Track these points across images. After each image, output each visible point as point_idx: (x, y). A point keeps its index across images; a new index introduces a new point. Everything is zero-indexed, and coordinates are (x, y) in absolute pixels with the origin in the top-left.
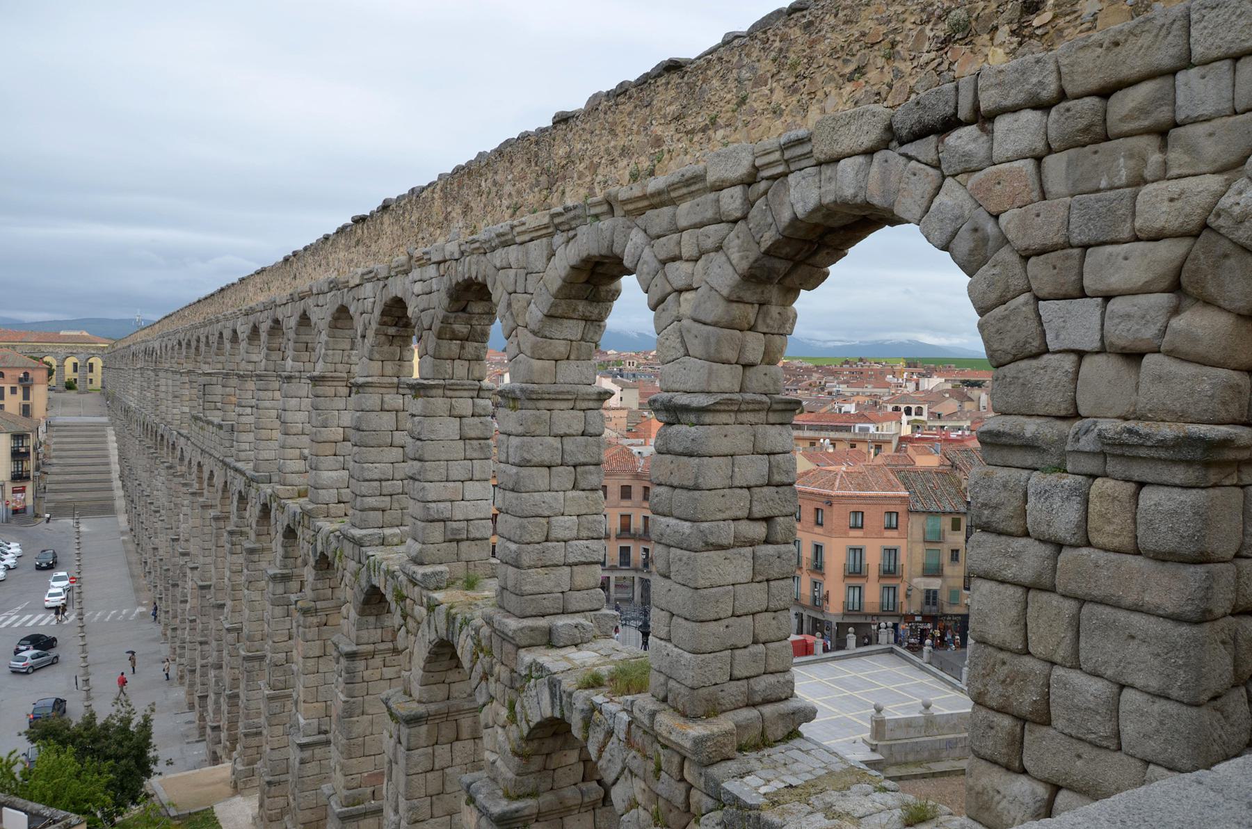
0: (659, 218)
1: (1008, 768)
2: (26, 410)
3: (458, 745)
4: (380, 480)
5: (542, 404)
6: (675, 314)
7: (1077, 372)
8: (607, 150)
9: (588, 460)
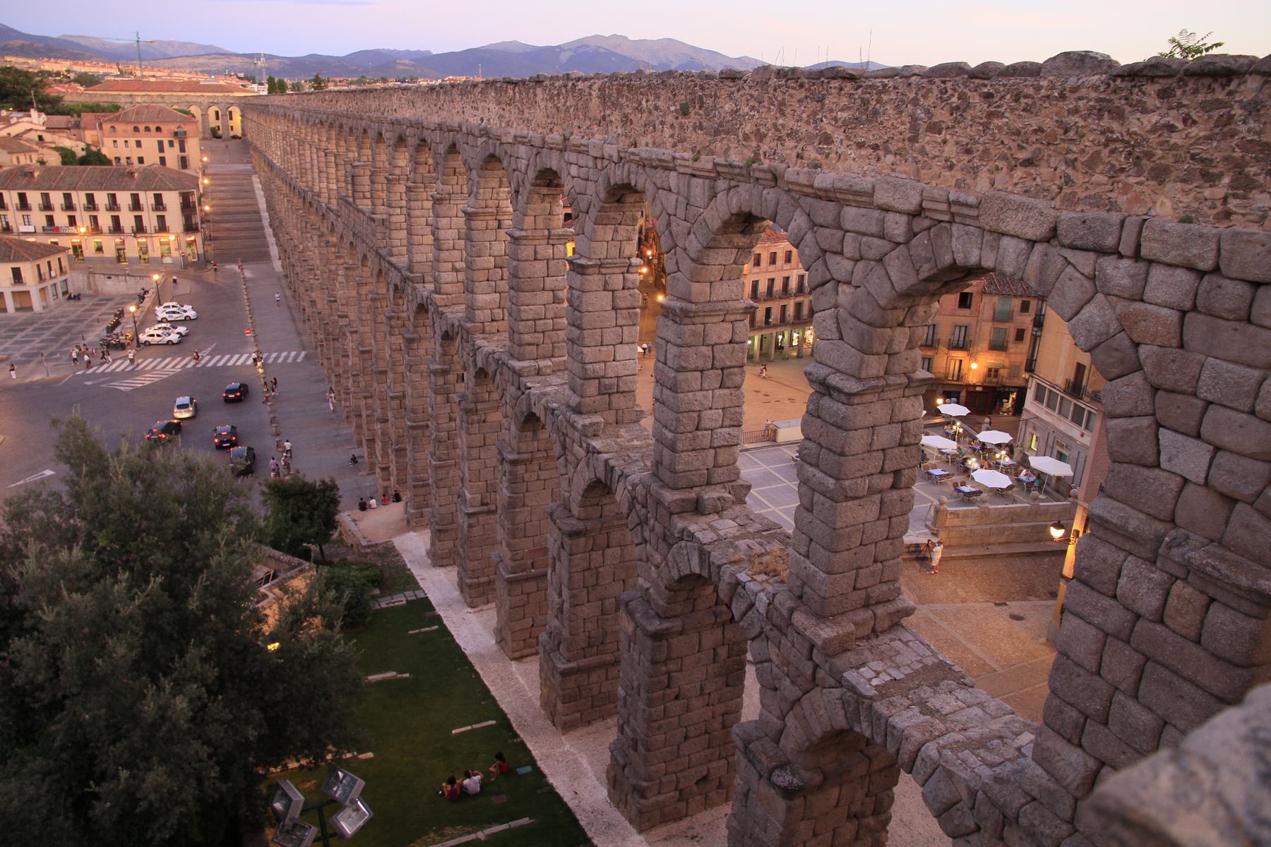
0: (826, 211)
1: (1069, 741)
2: (184, 162)
3: (608, 551)
4: (535, 320)
5: (696, 320)
6: (833, 302)
7: (1181, 491)
8: (775, 125)
9: (734, 363)
